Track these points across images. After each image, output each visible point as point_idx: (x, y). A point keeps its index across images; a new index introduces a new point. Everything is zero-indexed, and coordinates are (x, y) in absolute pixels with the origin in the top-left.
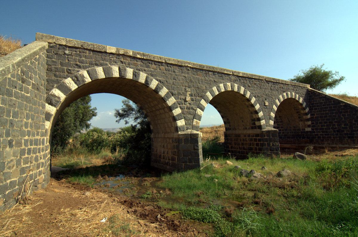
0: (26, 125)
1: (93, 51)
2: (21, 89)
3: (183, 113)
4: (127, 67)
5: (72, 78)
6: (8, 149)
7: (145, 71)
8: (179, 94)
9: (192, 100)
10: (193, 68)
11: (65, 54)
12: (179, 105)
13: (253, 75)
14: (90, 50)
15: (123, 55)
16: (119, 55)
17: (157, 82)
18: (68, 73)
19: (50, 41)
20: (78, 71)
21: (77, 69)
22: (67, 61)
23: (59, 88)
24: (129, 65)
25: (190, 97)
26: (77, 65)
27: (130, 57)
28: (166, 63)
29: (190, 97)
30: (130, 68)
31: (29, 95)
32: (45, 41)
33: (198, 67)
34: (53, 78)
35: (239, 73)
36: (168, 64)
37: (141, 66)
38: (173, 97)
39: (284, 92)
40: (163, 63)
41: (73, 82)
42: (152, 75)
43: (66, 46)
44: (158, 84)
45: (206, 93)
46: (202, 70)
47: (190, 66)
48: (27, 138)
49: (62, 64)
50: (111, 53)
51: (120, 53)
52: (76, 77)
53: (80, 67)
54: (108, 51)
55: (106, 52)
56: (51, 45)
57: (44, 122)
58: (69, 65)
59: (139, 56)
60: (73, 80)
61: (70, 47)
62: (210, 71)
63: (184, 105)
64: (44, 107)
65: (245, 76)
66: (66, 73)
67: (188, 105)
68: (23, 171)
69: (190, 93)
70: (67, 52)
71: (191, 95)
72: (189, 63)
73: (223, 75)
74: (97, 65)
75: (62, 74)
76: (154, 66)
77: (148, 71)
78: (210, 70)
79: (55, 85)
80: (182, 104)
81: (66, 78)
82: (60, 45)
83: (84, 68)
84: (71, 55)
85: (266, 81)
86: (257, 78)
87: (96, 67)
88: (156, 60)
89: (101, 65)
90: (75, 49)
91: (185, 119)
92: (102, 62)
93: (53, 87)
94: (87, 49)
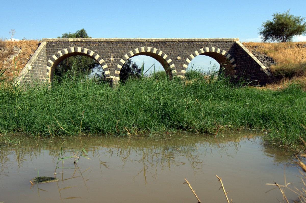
0: (40, 74)
1: (63, 42)
3: (108, 67)
4: (78, 47)
5: (55, 55)
7: (87, 47)
8: (106, 57)
9: (115, 60)
10: (116, 42)
11: (52, 45)
12: (106, 63)
13: (165, 40)
14: (62, 42)
15: (76, 41)
16: (74, 42)
18: (54, 53)
19: (47, 41)
20: (57, 52)
21: (57, 51)
22: (53, 48)
23: (51, 59)
24: (79, 46)
25: (113, 59)
26: (57, 49)
27: (79, 42)
28: (98, 42)
29: (113, 59)
30: (80, 47)
31: (41, 64)
32: (45, 42)
33: (119, 41)
34: (49, 56)
35: (152, 40)
36: (100, 42)
37: (85, 45)
38: (102, 59)
39: (201, 48)
40: (97, 42)
41: (56, 57)
42: (91, 49)
43: (53, 42)
44: (94, 53)
45: (124, 55)
46: (122, 42)
47: (113, 41)
48: (41, 78)
49: (51, 50)
51: (75, 41)
52: (57, 54)
53: (58, 50)
54: (69, 41)
55: (68, 42)
56: (48, 42)
57: (46, 73)
58: (54, 50)
60: (56, 56)
61: (54, 42)
62: (128, 42)
63: (109, 63)
64: (46, 67)
65: (157, 41)
66: (53, 53)
67: (112, 63)
69: (113, 56)
70: (53, 44)
71: (114, 57)
72: (113, 40)
73: (138, 43)
74: (65, 48)
75: (52, 53)
76: (92, 44)
77: (89, 47)
78: (128, 41)
79: (50, 58)
80: (108, 62)
81: (53, 55)
82: (51, 42)
83: (60, 50)
84: (55, 45)
85: (181, 42)
86: (170, 41)
87: (64, 49)
88: (93, 41)
89: (67, 48)
90: (56, 43)
91: (110, 70)
92: (67, 46)
93: (49, 59)
94: (61, 42)
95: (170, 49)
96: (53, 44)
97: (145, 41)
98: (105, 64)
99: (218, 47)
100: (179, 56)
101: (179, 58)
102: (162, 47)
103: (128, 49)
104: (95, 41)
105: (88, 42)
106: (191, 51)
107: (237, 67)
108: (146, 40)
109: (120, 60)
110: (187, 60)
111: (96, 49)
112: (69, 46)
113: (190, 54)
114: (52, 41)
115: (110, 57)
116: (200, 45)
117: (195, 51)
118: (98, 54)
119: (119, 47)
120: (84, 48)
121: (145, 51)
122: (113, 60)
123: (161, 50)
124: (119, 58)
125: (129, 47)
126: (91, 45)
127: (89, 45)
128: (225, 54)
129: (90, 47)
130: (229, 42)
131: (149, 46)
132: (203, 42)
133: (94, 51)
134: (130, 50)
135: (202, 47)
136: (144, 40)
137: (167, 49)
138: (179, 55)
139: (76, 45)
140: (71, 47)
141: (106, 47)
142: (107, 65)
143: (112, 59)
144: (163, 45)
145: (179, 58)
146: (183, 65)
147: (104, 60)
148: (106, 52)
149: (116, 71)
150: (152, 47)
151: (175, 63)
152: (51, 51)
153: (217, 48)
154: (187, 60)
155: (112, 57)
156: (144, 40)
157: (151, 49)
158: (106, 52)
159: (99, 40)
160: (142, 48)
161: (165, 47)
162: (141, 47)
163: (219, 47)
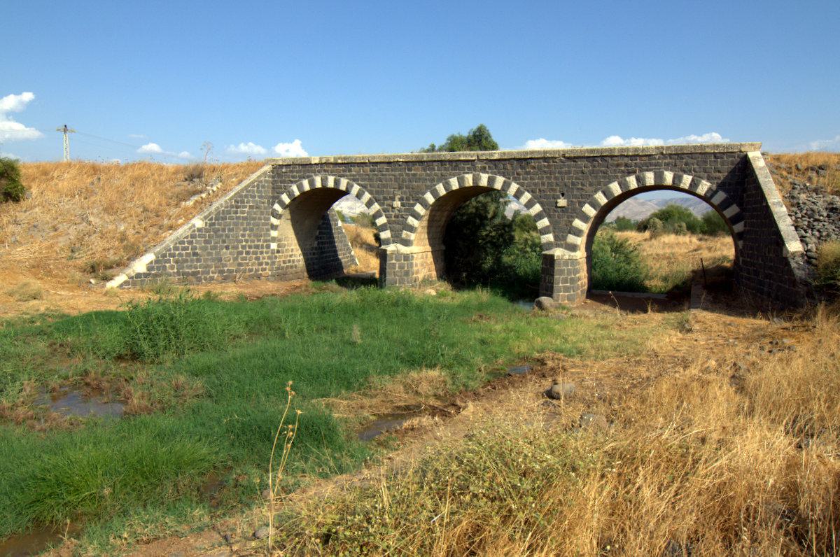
1: (302, 165)
2: (236, 213)
3: (389, 222)
6: (224, 250)
8: (385, 199)
9: (403, 205)
10: (406, 162)
12: (384, 213)
13: (527, 153)
14: (299, 165)
15: (325, 163)
16: (322, 164)
17: (359, 187)
24: (332, 173)
27: (331, 163)
28: (370, 163)
29: (399, 203)
30: (333, 175)
31: (246, 215)
33: (414, 160)
34: (276, 194)
36: (374, 163)
38: (376, 204)
39: (630, 173)
40: (366, 163)
41: (287, 197)
42: (354, 180)
43: (283, 165)
44: (360, 190)
45: (424, 193)
46: (422, 162)
47: (401, 160)
48: (244, 243)
50: (315, 164)
52: (289, 192)
53: (292, 182)
54: (313, 163)
55: (311, 164)
59: (340, 161)
61: (286, 165)
62: (435, 161)
63: (391, 213)
64: (269, 219)
65: (506, 157)
67: (397, 212)
68: (240, 265)
69: (399, 196)
71: (401, 199)
72: (400, 157)
73: (458, 163)
74: (304, 178)
75: (280, 190)
76: (357, 168)
77: (351, 175)
78: (434, 159)
80: (388, 211)
82: (279, 165)
83: (295, 182)
85: (569, 158)
86: (539, 156)
88: (358, 161)
89: (308, 177)
91: (391, 231)
93: (274, 202)
95: (539, 179)
96: (284, 170)
97: (474, 158)
98: (381, 216)
99: (685, 172)
100: (562, 198)
101: (562, 202)
102: (517, 174)
103: (432, 180)
104: (362, 161)
105: (348, 163)
106: (599, 183)
107: (745, 230)
108: (478, 156)
109: (414, 205)
110: (584, 209)
111: (363, 180)
112: (313, 174)
113: (596, 192)
114: (281, 163)
115: (393, 199)
116: (626, 165)
117: (610, 183)
118: (367, 191)
119: (414, 175)
120: (341, 177)
121: (473, 183)
122: (399, 206)
123: (515, 180)
124: (412, 202)
125: (436, 175)
126: (355, 170)
127: (350, 171)
128: (707, 192)
129: (353, 175)
130: (723, 153)
131: (484, 170)
132: (638, 155)
133: (359, 185)
134: (439, 181)
135: (634, 172)
136: (472, 157)
137: (531, 179)
138: (563, 195)
139: (325, 171)
140: (316, 175)
141: (385, 175)
142: (387, 217)
143: (397, 204)
144: (522, 168)
145: (562, 202)
146: (572, 222)
147: (380, 205)
148: (384, 186)
149: (405, 232)
150: (491, 173)
151: (549, 217)
152: (279, 184)
153: (681, 173)
154: (584, 209)
155: (397, 197)
156: (472, 157)
157: (489, 178)
158: (384, 186)
159: (370, 159)
160: (467, 176)
161: (527, 173)
162: (464, 173)
163: (688, 172)
